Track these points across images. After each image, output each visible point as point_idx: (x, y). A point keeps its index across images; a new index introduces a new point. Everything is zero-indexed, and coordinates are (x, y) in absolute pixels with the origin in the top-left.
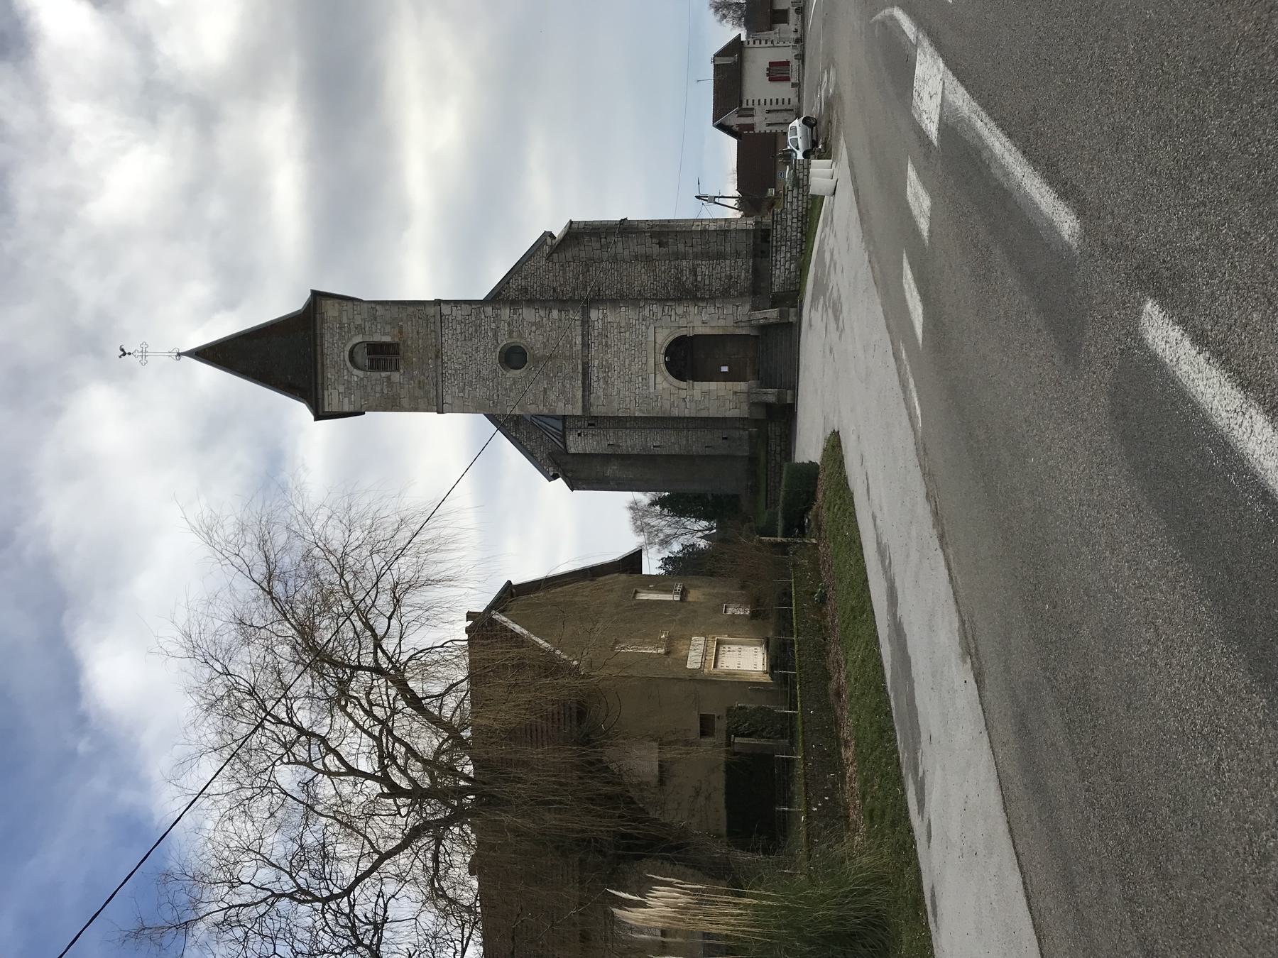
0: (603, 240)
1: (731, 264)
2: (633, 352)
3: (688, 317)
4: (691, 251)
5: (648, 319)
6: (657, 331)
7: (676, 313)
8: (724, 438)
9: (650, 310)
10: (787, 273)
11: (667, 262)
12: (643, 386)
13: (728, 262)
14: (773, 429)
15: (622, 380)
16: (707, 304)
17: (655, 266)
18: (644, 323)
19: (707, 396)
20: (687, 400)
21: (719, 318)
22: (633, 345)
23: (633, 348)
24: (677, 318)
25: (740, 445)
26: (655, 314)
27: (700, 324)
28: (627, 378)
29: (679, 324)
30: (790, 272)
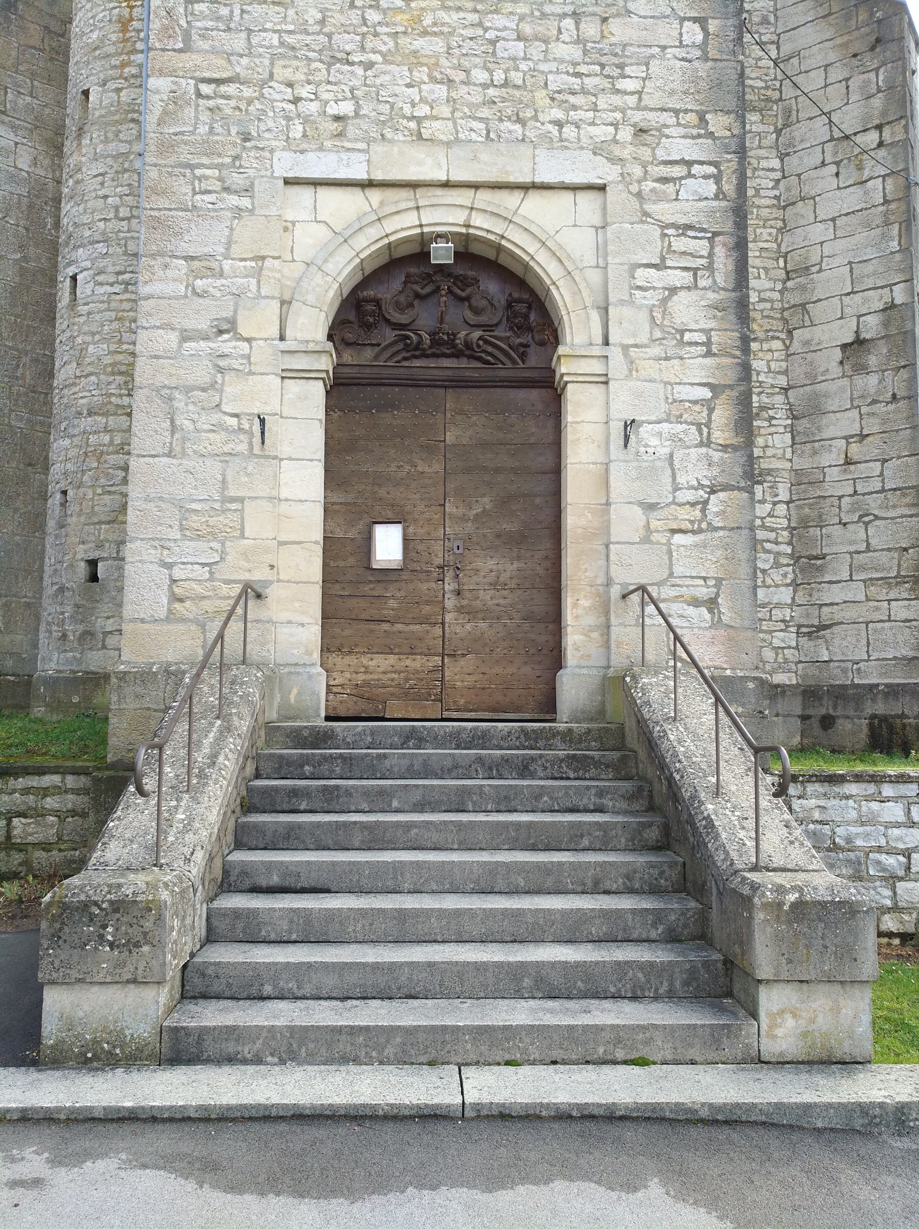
0: (872, 137)
1: (778, 605)
2: (480, 76)
3: (656, 351)
4: (826, 459)
5: (645, 153)
6: (582, 197)
7: (673, 290)
8: (93, 564)
9: (689, 164)
10: (890, 861)
11: (782, 381)
12: (306, 120)
13: (785, 595)
14: (50, 802)
15: (336, 19)
16: (725, 448)
17: (767, 340)
18: (626, 134)
19: (243, 448)
20: (225, 344)
21: (651, 507)
22: (516, 78)
23: (499, 76)
24: (652, 298)
25: (64, 636)
26: (670, 188)
27: (622, 410)
28: (347, 41)
29: (622, 302)
30: (892, 880)
